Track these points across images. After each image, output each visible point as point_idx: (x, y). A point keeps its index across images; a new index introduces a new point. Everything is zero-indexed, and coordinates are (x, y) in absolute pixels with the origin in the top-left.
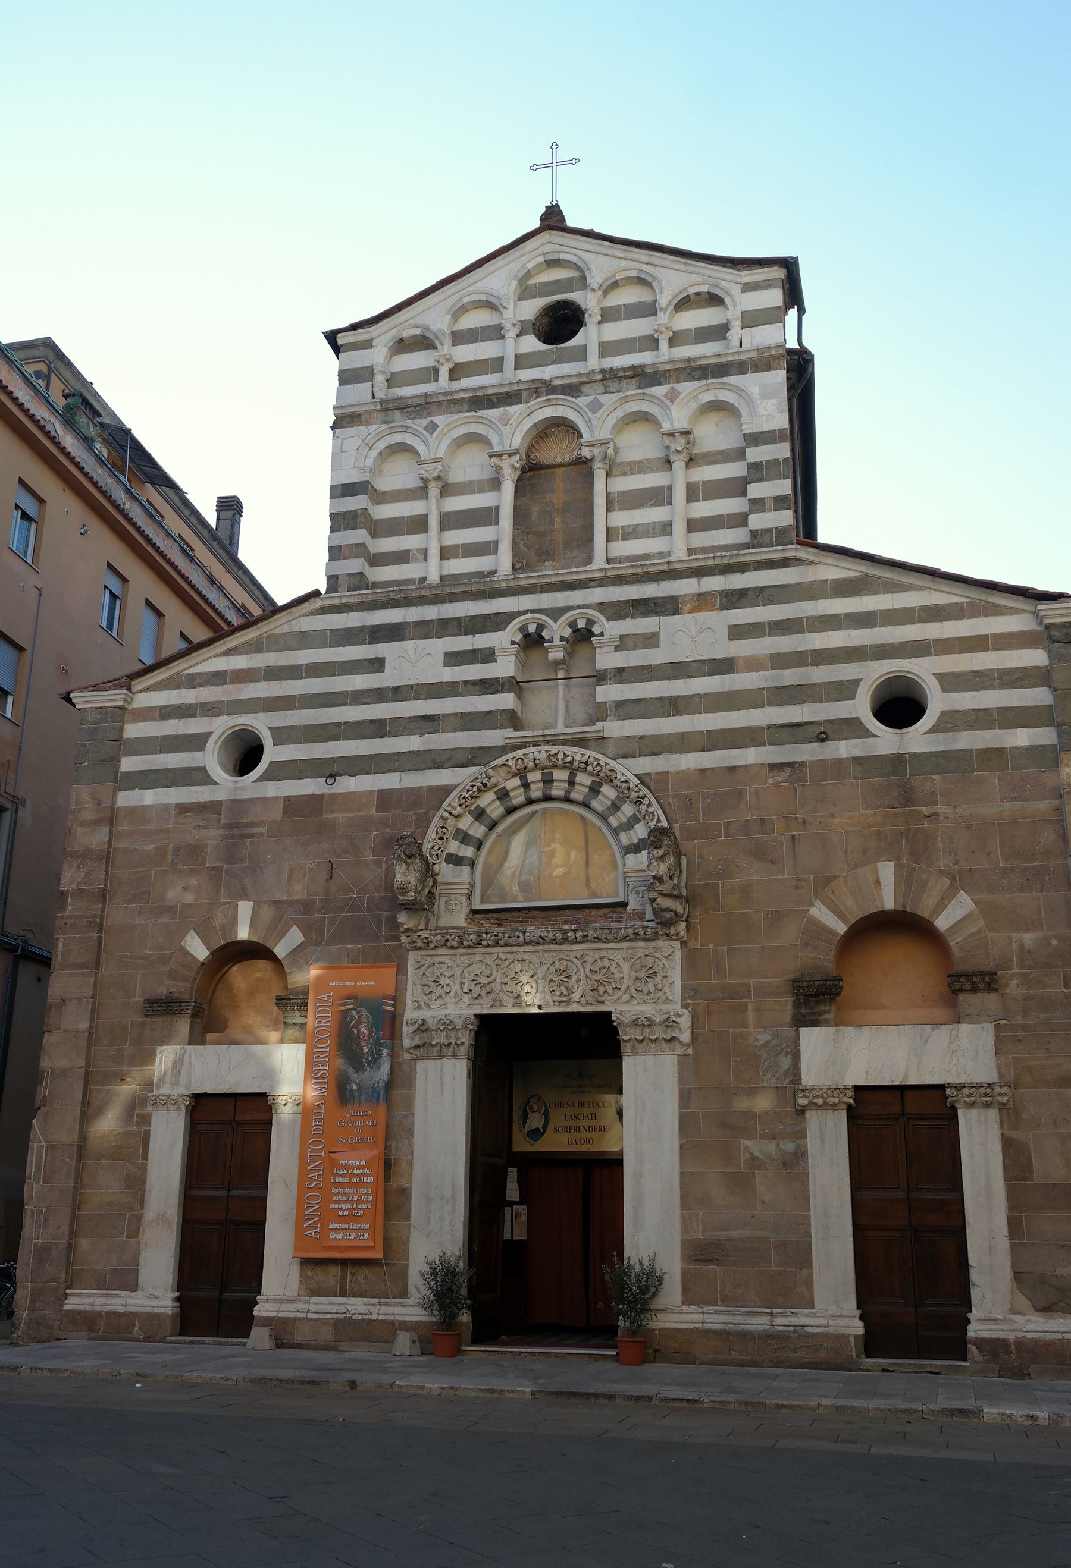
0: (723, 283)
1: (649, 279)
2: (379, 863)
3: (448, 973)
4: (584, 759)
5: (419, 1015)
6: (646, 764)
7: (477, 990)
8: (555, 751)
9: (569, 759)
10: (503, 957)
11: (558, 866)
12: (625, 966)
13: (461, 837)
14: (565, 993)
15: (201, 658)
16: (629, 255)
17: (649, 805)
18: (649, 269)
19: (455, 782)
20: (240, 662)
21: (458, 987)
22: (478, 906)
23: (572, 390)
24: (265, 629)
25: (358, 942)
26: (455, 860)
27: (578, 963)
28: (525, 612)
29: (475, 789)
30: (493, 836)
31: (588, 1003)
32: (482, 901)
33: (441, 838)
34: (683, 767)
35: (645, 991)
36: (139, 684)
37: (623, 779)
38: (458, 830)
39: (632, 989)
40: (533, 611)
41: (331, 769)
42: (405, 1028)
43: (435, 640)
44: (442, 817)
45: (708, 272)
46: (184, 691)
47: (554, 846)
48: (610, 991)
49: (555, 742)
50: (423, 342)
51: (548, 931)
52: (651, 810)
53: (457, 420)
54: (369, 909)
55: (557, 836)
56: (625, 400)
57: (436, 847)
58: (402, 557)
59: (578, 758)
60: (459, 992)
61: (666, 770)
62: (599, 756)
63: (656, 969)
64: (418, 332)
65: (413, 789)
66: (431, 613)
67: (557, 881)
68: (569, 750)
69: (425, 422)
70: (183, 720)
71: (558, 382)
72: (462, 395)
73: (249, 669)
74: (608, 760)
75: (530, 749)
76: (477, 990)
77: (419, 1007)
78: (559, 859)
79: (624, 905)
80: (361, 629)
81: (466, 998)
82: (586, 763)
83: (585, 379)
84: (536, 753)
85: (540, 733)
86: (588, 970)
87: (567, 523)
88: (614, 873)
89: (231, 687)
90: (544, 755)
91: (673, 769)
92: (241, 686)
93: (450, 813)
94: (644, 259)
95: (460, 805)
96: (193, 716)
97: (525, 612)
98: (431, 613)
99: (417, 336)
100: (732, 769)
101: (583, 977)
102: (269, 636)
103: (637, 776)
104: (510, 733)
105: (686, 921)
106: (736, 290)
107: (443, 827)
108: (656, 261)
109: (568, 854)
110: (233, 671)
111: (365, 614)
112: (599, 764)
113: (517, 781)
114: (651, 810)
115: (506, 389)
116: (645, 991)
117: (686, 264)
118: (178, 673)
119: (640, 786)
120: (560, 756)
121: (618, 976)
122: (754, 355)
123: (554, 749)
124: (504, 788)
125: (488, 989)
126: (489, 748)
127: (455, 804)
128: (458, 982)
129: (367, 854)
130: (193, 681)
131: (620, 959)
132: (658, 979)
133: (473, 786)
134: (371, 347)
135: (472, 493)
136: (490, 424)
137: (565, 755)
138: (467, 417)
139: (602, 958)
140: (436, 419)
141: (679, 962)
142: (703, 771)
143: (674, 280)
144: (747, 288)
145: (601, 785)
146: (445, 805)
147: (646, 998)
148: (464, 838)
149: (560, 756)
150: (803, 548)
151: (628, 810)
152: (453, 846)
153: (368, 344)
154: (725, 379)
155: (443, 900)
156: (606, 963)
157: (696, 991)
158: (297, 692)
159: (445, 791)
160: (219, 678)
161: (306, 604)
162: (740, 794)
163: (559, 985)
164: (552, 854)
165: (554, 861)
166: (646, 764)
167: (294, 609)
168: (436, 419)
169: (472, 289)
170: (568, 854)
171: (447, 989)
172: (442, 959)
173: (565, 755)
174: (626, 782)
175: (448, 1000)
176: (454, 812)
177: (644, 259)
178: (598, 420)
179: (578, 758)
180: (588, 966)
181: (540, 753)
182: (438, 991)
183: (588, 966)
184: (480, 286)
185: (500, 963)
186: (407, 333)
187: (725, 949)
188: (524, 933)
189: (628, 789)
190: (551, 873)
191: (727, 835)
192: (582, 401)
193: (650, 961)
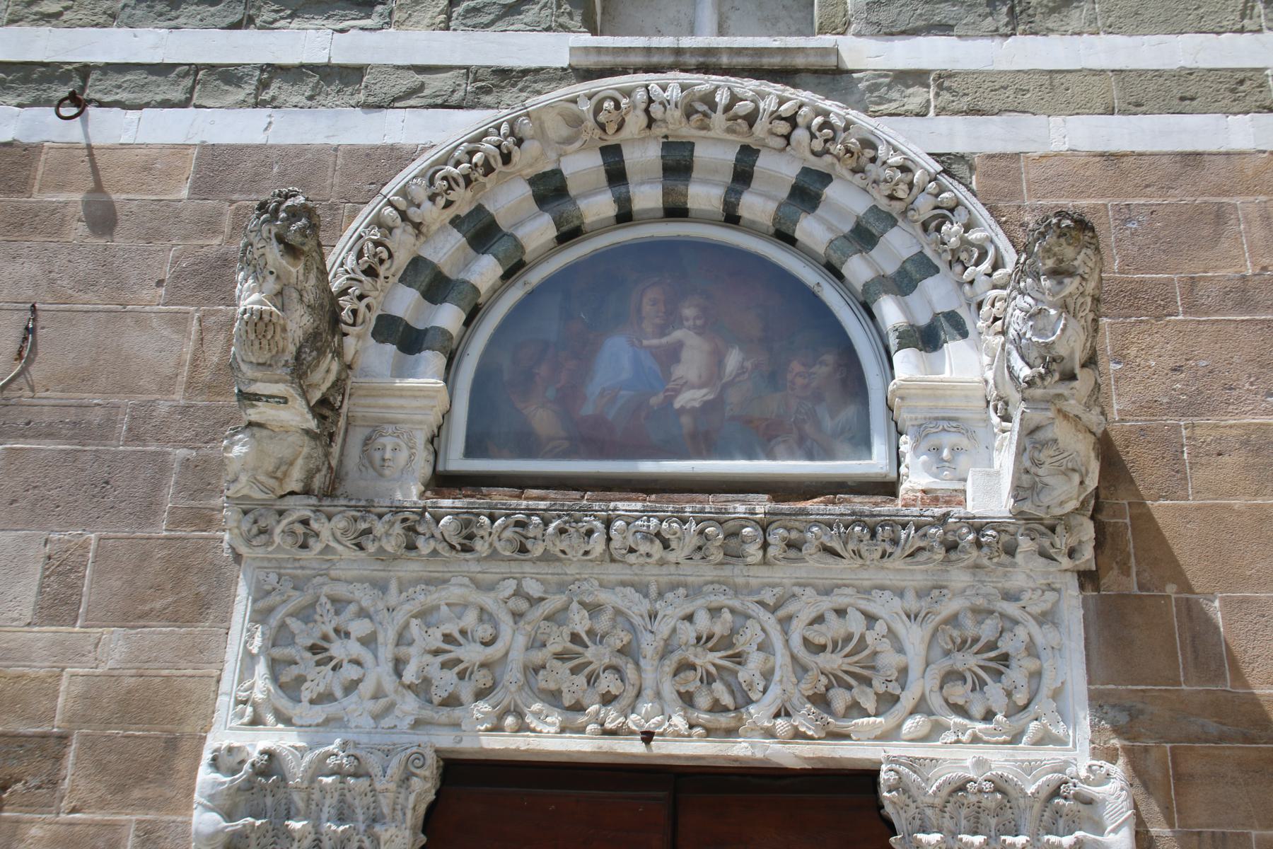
2: (178, 322)
3: (359, 628)
4: (786, 109)
5: (256, 743)
6: (961, 134)
7: (446, 681)
8: (706, 87)
9: (743, 107)
10: (533, 588)
11: (687, 385)
12: (915, 638)
13: (425, 278)
14: (727, 700)
17: (968, 227)
19: (421, 139)
21: (386, 668)
22: (456, 462)
25: (88, 524)
26: (409, 340)
27: (770, 621)
29: (477, 158)
30: (515, 294)
31: (798, 735)
32: (470, 452)
33: (371, 272)
34: (1058, 145)
35: (977, 710)
37: (896, 160)
38: (417, 263)
39: (936, 701)
41: (74, 87)
42: (205, 775)
44: (378, 222)
47: (678, 334)
48: (869, 704)
49: (704, 69)
51: (684, 521)
52: (974, 235)
54: (135, 436)
55: (689, 312)
57: (355, 290)
59: (768, 105)
60: (389, 683)
61: (1010, 149)
62: (828, 105)
63: (1005, 645)
65: (301, 150)
67: (686, 421)
68: (748, 86)
74: (853, 114)
75: (641, 78)
76: (446, 681)
77: (256, 721)
78: (692, 364)
79: (888, 488)
81: (410, 705)
82: (792, 120)
84: (654, 88)
85: (667, 42)
86: (796, 641)
88: (849, 412)
90: (674, 93)
91: (1036, 149)
93: (404, 216)
95: (432, 198)
100: (1192, 159)
101: (781, 659)
103: (935, 156)
104: (587, 39)
105: (1092, 518)
107: (377, 244)
109: (718, 360)
112: (826, 124)
113: (594, 161)
114: (974, 235)
116: (977, 710)
119: (945, 180)
120: (722, 98)
121: (889, 660)
123: (703, 83)
124: (557, 173)
125: (482, 679)
126: (525, 72)
127: (420, 192)
128: (386, 652)
129: (146, 294)
131: (897, 614)
132: (1016, 675)
133: (471, 153)
137: (734, 99)
139: (841, 613)
141: (1078, 630)
142: (1111, 158)
145: (826, 179)
146: (391, 189)
147: (980, 726)
148: (437, 287)
149: (722, 98)
151: (899, 245)
152: (406, 303)
155: (357, 437)
156: (855, 624)
157: (1134, 714)
159: (397, 157)
162: (1220, 216)
163: (708, 679)
164: (673, 354)
165: (680, 371)
166: (961, 134)
170: (718, 360)
171: (351, 672)
172: (341, 590)
173: (734, 99)
174: (904, 169)
175: (351, 702)
176: (412, 212)
179: (768, 105)
180: (798, 630)
181: (672, 85)
182: (320, 679)
183: (798, 630)
185: (523, 605)
187: (1217, 603)
188: (608, 523)
189: (911, 185)
190: (669, 401)
191: (1191, 308)
193: (987, 630)
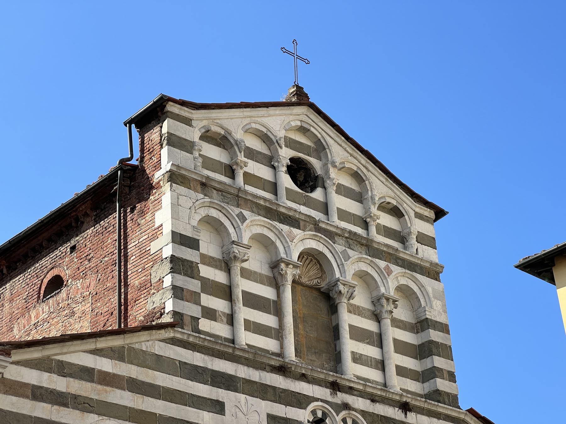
0: (405, 205)
1: (364, 178)
15: (72, 349)
16: (355, 154)
18: (364, 170)
20: (105, 365)
23: (331, 235)
24: (128, 341)
28: (317, 400)
36: (17, 355)
40: (322, 401)
43: (258, 400)
45: (398, 193)
46: (55, 377)
50: (223, 141)
53: (259, 220)
56: (360, 260)
58: (210, 314)
64: (223, 132)
66: (255, 375)
69: (237, 211)
70: (56, 407)
71: (323, 226)
72: (262, 202)
73: (114, 375)
80: (205, 370)
83: (339, 232)
87: (307, 332)
89: (99, 387)
92: (108, 389)
94: (363, 162)
96: (66, 405)
97: (317, 400)
98: (255, 375)
99: (220, 134)
102: (131, 349)
106: (412, 214)
108: (370, 168)
110: (100, 372)
111: (206, 358)
115: (291, 213)
117: (387, 180)
118: (48, 357)
122: (427, 265)
130: (63, 369)
134: (190, 125)
135: (256, 281)
136: (279, 235)
138: (264, 221)
140: (246, 213)
143: (380, 188)
144: (419, 216)
150: (471, 416)
153: (188, 122)
154: (415, 274)
158: (158, 411)
160: (87, 374)
161: (163, 331)
167: (154, 332)
168: (246, 213)
169: (259, 120)
177: (363, 162)
178: (349, 267)
184: (265, 120)
186: (214, 129)
192: (339, 248)
